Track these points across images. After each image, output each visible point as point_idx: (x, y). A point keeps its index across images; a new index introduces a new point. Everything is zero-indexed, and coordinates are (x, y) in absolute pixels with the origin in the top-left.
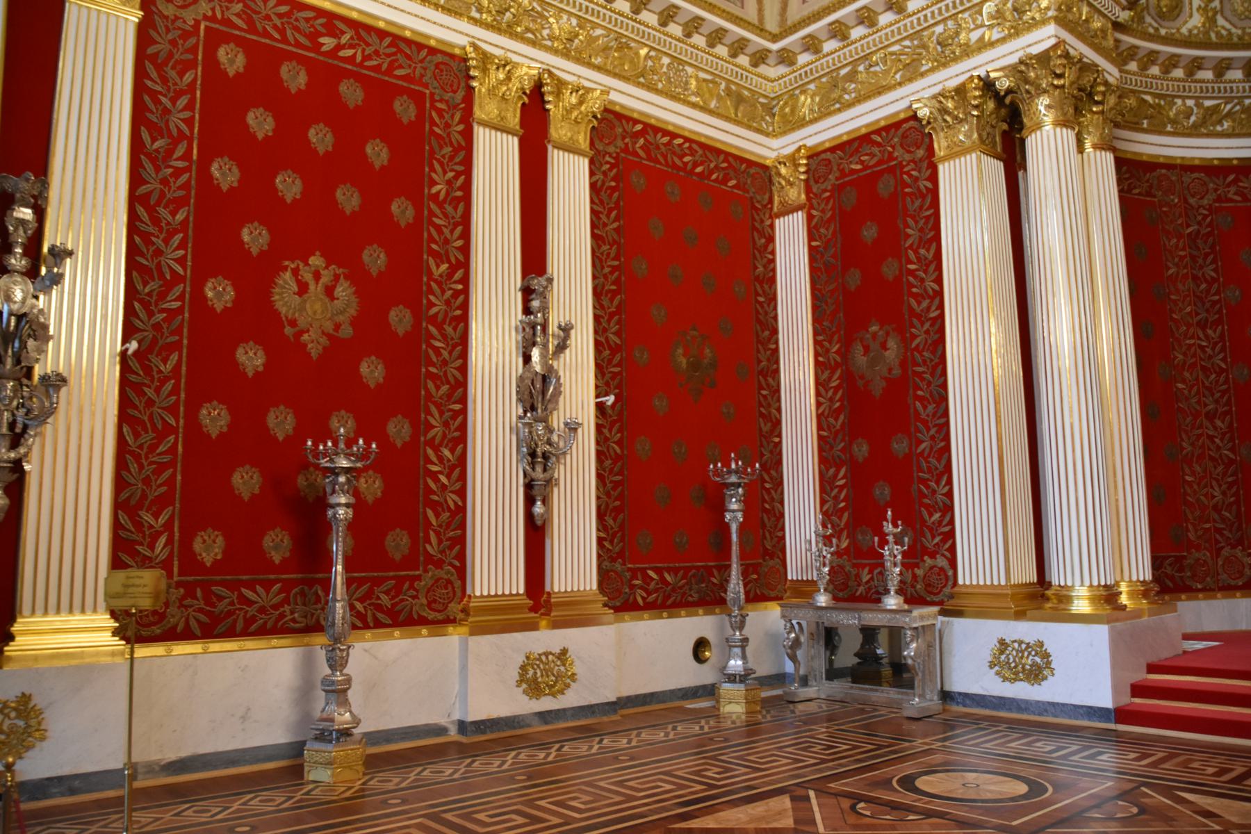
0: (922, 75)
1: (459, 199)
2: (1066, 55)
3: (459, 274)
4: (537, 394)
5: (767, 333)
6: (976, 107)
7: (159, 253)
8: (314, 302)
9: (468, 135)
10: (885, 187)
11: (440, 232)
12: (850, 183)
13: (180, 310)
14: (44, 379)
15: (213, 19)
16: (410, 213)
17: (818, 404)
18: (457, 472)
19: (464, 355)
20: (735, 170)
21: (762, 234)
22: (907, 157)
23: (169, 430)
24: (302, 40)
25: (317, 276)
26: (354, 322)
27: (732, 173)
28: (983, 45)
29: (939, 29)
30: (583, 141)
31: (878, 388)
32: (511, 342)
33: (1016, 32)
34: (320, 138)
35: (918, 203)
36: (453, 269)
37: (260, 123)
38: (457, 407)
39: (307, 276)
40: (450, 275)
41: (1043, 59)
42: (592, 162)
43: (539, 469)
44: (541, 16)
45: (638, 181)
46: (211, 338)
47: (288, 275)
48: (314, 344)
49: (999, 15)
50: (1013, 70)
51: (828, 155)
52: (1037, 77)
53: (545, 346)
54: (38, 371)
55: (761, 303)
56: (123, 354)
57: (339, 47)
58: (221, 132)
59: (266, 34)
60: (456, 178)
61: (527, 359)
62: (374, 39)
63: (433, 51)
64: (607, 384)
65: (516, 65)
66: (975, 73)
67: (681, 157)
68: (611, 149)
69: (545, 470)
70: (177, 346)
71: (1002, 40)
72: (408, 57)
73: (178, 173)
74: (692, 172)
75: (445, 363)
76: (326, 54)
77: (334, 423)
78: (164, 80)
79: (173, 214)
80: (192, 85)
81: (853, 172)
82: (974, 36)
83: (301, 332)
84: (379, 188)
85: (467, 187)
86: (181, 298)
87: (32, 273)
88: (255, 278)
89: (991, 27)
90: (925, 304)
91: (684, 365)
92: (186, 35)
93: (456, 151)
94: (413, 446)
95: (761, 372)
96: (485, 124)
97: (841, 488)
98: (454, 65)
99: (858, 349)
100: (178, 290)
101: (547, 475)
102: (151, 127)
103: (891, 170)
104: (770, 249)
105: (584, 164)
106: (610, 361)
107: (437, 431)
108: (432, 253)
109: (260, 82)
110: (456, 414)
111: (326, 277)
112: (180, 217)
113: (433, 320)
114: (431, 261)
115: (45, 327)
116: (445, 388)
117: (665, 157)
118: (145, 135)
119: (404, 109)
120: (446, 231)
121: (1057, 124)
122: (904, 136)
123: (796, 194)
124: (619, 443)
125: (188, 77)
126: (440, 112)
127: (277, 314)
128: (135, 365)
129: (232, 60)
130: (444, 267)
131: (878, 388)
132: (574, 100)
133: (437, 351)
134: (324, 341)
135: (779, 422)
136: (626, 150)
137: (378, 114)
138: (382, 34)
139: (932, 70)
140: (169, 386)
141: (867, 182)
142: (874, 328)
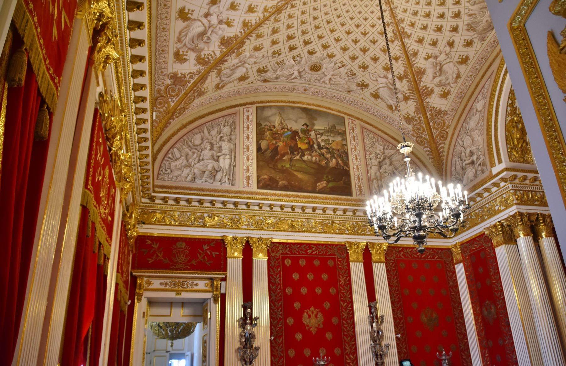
0: (486, 220)
1: (348, 284)
2: (521, 214)
3: (350, 305)
4: (377, 337)
5: (457, 305)
6: (501, 231)
7: (276, 313)
8: (313, 320)
9: (349, 266)
10: (482, 255)
11: (344, 294)
12: (473, 254)
13: (282, 327)
14: (255, 348)
15: (283, 254)
16: (335, 291)
17: (477, 328)
18: (355, 362)
19: (354, 328)
20: (437, 253)
21: (450, 271)
22: (486, 246)
23: (282, 357)
24: (304, 252)
25: (313, 313)
26: (323, 323)
27: (436, 254)
28: (500, 211)
29: (487, 206)
30: (383, 259)
31: (491, 322)
32: (367, 322)
33: (508, 207)
34: (310, 276)
35: (492, 261)
36: (348, 304)
37: (296, 276)
38: (353, 343)
39: (310, 313)
40: (347, 306)
41: (514, 216)
42: (386, 264)
43: (379, 359)
44: (366, 226)
45: (402, 265)
46: (289, 332)
47: (305, 314)
48: (314, 331)
49: (501, 202)
50: (506, 219)
51: (466, 245)
52: (515, 222)
53: (378, 322)
54: (254, 346)
55: (453, 295)
56: (271, 340)
57: (313, 252)
58: (288, 281)
59: (295, 254)
60: (346, 278)
61: (372, 327)
62: (321, 247)
63: (336, 245)
64: (399, 330)
65: (359, 243)
66: (497, 221)
67: (416, 254)
68: (392, 258)
69: (381, 359)
70: (282, 336)
71: (504, 210)
72: (330, 249)
73: (279, 293)
74: (421, 258)
75: (348, 331)
76: (310, 254)
77: (320, 351)
78: (274, 271)
79: (278, 303)
80: (280, 271)
81: (474, 250)
82: (497, 208)
83: (310, 328)
84: (326, 286)
85: (350, 280)
86: (282, 324)
87: (251, 324)
88: (298, 316)
89: (500, 206)
90: (499, 294)
91: (426, 320)
92: (277, 259)
93: (346, 271)
94: (342, 355)
95: (456, 318)
96: (353, 261)
97: (487, 357)
98: (343, 247)
99: (484, 309)
100: (281, 322)
101: (382, 361)
102: (272, 283)
103: (483, 250)
104: (454, 275)
105: (384, 265)
106: (399, 323)
107: (348, 351)
108: (342, 301)
109: (295, 266)
110: (353, 345)
111: (315, 313)
112: (280, 304)
113: (344, 319)
114: (342, 303)
115: (255, 336)
116: (349, 338)
117: (411, 256)
118: (271, 286)
119: (331, 263)
120: (345, 294)
121: (524, 235)
122: (484, 239)
123: (459, 257)
124: (406, 348)
125: (279, 269)
126: (340, 261)
127: (304, 324)
128: (273, 342)
129: (288, 262)
130: (346, 304)
131: (491, 322)
132: (378, 247)
133: (346, 328)
134: (316, 329)
135: (466, 334)
136: (397, 257)
137: (324, 267)
138: (323, 245)
139: (488, 219)
140: (281, 346)
141: (477, 254)
142: (487, 302)
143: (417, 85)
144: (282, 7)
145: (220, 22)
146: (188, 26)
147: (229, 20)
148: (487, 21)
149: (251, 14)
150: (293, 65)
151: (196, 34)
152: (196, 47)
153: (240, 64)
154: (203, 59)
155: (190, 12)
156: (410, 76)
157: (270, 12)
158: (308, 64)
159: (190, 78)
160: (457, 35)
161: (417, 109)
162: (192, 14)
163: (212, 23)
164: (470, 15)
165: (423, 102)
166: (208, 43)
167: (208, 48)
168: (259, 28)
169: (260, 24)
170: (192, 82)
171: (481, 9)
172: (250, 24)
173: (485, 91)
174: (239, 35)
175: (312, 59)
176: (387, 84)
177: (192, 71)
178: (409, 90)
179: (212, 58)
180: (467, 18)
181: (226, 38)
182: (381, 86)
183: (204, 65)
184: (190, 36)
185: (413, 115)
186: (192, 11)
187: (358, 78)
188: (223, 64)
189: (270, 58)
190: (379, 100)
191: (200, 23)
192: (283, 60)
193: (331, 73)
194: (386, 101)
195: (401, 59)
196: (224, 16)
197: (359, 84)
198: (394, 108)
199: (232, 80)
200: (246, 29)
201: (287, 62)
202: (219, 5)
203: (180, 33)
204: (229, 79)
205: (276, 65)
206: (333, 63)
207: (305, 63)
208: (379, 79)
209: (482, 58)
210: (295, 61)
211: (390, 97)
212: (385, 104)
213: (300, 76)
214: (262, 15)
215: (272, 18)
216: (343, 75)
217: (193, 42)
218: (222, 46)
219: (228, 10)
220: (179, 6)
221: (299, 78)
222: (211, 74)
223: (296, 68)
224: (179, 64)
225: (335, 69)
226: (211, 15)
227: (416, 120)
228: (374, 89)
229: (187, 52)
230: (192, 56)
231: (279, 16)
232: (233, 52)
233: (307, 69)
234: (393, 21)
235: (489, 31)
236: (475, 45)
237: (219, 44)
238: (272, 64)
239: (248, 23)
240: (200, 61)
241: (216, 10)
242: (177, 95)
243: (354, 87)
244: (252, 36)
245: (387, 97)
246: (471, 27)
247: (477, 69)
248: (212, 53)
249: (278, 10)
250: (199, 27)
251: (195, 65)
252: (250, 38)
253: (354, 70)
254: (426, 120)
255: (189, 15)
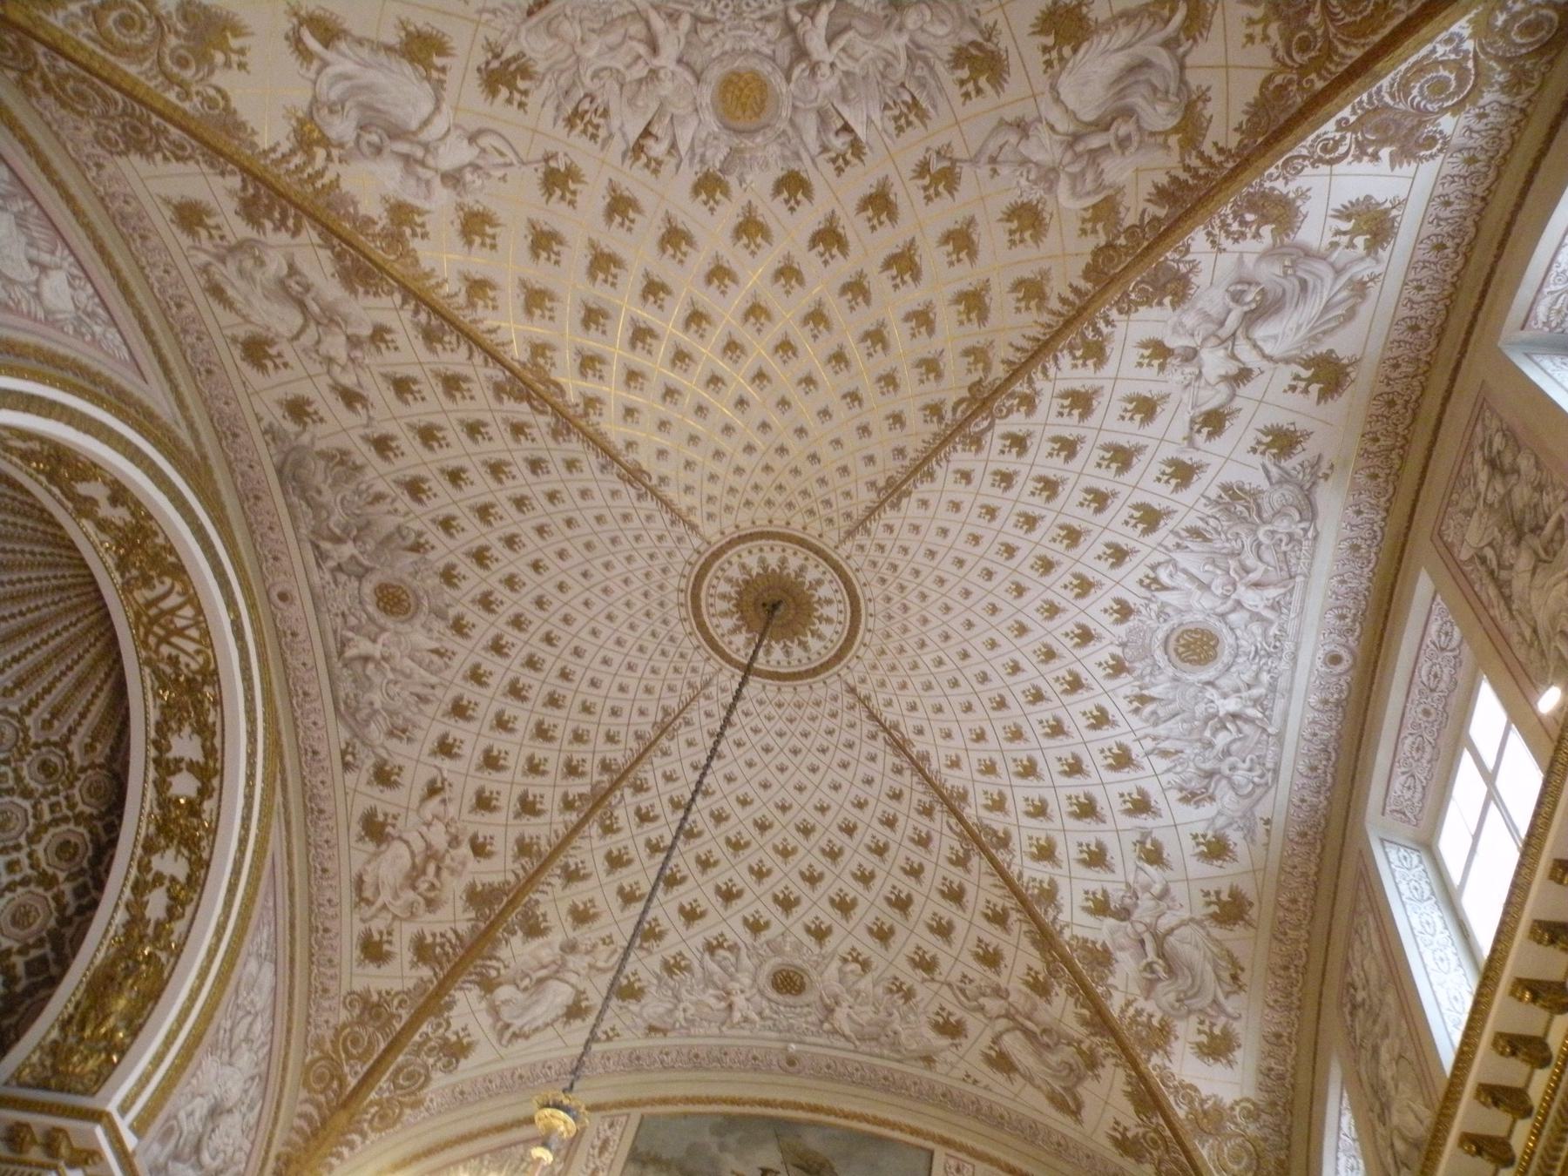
143: (329, 232)
144: (974, 414)
145: (1191, 355)
146: (1315, 339)
147: (1156, 363)
148: (319, 492)
149: (1077, 385)
150: (845, 99)
151: (1287, 311)
152: (1294, 265)
153: (1096, 142)
154: (1264, 219)
155: (1302, 384)
156: (376, 248)
157: (1012, 396)
158: (786, 113)
159: (1337, 143)
160: (362, 431)
161: (232, 124)
162: (1297, 377)
163: (1221, 353)
164: (379, 497)
165: (244, 170)
166: (1240, 282)
167: (1241, 261)
168: (1037, 332)
169: (1040, 352)
170: (1329, 128)
171: (369, 523)
172: (1078, 353)
173: (98, 329)
174: (1114, 314)
175: (774, 149)
176: (426, 147)
177: (1324, 169)
178: (335, 184)
179: (1224, 225)
180: (380, 487)
181: (1167, 300)
182: (439, 126)
183: (1264, 195)
184: (1313, 307)
185: (219, 78)
186: (1293, 388)
187: (549, 111)
188: (1175, 180)
189: (959, 152)
190: (393, 37)
191: (1268, 350)
192: (900, 129)
193: (666, 88)
194: (365, 53)
195: (462, 300)
196: (1176, 375)
197: (525, 73)
198: (313, 44)
199: (1125, 34)
200: (1090, 334)
201: (876, 116)
202: (1197, 411)
203: (1351, 314)
204: (1140, 50)
205: (924, 104)
206: (683, 147)
207: (799, 120)
208: (466, 154)
209: (209, 372)
210: (847, 128)
211: (368, 88)
212: (357, 32)
213: (791, 29)
214: (1038, 385)
215: (999, 372)
216: (609, 94)
217: (1304, 285)
218: (1183, 269)
219: (1165, 397)
220: (1339, 405)
221: (796, 17)
222: (1233, 141)
223: (829, 82)
224: (1379, 197)
225: (660, 112)
226: (1225, 378)
227: (183, 63)
228: (452, 79)
229: (1334, 245)
230: (1313, 230)
231: (975, 377)
232: (1131, 231)
233: (777, 80)
234: (583, 423)
235: (284, 462)
236: (278, 412)
237: (1194, 279)
238: (943, 106)
239: (1085, 358)
240: (1282, 213)
241: (1205, 394)
242: (1420, 69)
243: (536, 46)
244: (1064, 301)
245: (371, 76)
246: (341, 461)
247: (185, 331)
248: (1227, 243)
249: (984, 402)
250: (1275, 337)
251: (1303, 195)
252: (1072, 297)
253: (584, 142)
254: (159, 105)
255: (1306, 374)
